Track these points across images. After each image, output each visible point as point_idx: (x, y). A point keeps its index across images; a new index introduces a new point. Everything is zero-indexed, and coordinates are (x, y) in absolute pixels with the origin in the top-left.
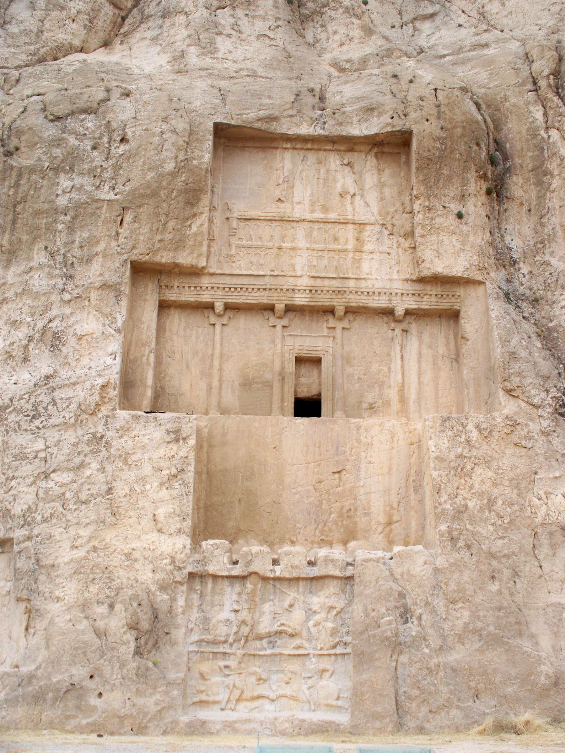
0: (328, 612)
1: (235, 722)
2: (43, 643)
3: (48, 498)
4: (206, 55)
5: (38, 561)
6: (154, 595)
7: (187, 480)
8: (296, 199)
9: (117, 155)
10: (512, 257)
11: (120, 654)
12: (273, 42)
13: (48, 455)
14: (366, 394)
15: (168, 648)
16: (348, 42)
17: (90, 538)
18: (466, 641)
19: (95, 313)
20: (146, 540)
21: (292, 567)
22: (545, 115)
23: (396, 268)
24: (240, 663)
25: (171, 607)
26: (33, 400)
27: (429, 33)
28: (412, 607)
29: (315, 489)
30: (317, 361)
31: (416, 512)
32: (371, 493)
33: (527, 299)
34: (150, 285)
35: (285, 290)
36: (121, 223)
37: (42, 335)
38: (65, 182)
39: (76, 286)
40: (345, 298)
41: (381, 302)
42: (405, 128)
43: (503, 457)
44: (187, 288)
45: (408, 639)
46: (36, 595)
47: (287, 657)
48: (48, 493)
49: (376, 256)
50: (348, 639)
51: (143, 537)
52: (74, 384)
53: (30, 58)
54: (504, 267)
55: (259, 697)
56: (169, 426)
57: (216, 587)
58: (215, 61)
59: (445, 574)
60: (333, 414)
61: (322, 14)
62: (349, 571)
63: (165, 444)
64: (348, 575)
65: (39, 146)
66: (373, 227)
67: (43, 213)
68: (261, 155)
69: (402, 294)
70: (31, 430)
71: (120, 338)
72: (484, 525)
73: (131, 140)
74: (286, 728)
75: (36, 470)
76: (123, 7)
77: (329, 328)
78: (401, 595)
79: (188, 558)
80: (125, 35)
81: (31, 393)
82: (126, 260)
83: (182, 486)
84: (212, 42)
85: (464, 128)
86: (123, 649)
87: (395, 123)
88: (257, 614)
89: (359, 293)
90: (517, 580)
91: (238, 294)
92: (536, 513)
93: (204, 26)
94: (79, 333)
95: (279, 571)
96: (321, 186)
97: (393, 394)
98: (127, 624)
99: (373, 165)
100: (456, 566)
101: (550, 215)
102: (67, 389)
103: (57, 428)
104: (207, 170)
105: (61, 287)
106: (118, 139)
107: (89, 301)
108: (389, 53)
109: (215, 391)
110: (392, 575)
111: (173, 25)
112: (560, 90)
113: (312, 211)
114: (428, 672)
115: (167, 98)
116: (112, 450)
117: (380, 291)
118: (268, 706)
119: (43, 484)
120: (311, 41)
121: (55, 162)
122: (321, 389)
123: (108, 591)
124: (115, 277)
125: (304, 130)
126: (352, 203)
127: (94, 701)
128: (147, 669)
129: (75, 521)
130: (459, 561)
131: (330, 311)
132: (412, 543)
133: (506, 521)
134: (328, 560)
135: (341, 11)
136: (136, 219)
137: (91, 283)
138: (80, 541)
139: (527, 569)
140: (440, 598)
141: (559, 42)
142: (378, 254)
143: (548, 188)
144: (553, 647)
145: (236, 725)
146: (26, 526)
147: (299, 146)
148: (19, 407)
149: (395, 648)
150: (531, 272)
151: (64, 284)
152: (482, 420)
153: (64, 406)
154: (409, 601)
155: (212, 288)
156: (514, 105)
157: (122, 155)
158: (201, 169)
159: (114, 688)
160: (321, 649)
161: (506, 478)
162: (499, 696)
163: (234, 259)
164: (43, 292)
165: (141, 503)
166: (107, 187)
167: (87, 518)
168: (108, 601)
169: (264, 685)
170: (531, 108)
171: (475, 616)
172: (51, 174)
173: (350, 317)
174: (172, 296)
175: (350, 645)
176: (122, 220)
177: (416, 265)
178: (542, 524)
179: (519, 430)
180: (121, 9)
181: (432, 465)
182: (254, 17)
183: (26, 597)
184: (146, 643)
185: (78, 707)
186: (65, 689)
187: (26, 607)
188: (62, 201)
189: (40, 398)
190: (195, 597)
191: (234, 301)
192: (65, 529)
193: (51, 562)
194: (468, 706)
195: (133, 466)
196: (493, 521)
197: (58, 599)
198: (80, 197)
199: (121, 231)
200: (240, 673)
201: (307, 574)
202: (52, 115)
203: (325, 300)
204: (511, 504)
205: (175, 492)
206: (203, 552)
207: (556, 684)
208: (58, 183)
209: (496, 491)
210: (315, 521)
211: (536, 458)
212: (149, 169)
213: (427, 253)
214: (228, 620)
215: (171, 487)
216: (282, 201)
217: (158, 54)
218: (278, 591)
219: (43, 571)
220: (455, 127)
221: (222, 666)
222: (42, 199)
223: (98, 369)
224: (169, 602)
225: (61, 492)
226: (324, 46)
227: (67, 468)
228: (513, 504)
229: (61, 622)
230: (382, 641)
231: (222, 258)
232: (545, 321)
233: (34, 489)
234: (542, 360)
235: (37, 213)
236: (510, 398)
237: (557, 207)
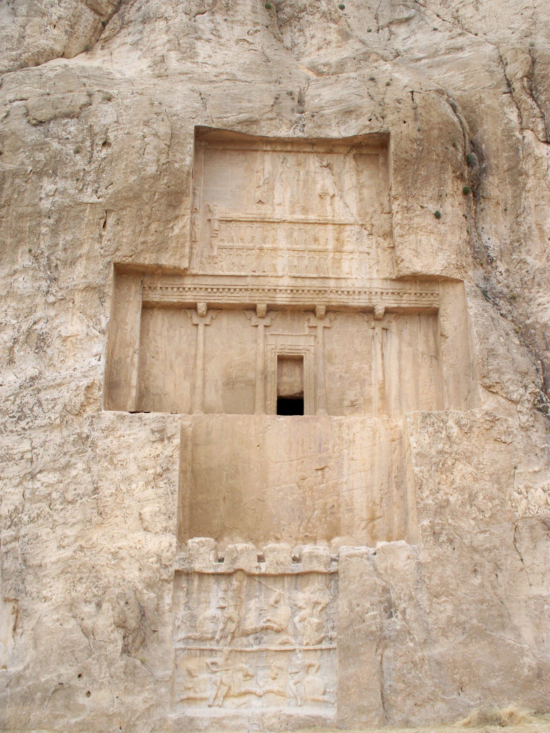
0: (314, 608)
1: (223, 718)
2: (31, 642)
3: (34, 498)
4: (186, 60)
5: (25, 561)
6: (141, 593)
7: (173, 479)
8: (276, 201)
9: (99, 159)
10: (489, 256)
11: (108, 653)
12: (252, 47)
13: (34, 455)
14: (348, 392)
15: (156, 646)
16: (325, 46)
17: (77, 538)
18: (450, 634)
19: (79, 314)
20: (133, 538)
21: (277, 563)
22: (520, 116)
23: (376, 268)
24: (227, 659)
25: (158, 605)
26: (18, 402)
27: (405, 37)
28: (396, 602)
29: (299, 486)
30: (299, 360)
31: (398, 507)
32: (353, 489)
33: (505, 296)
34: (133, 286)
35: (266, 290)
36: (104, 226)
37: (27, 337)
38: (48, 185)
39: (60, 289)
40: (326, 298)
41: (362, 301)
42: (382, 130)
43: (483, 452)
44: (170, 290)
45: (392, 634)
46: (24, 595)
47: (273, 653)
48: (34, 494)
49: (356, 256)
50: (333, 634)
51: (130, 536)
52: (60, 385)
53: (12, 63)
54: (482, 265)
55: (246, 693)
56: (154, 426)
57: (202, 585)
58: (195, 65)
59: (428, 568)
60: (315, 411)
61: (300, 18)
62: (334, 567)
63: (150, 443)
64: (332, 571)
65: (22, 150)
66: (352, 228)
67: (27, 216)
68: (242, 157)
69: (382, 293)
70: (17, 431)
71: (104, 339)
72: (465, 519)
73: (113, 144)
74: (274, 724)
75: (22, 470)
76: (103, 13)
77: (310, 327)
78: (386, 590)
79: (175, 556)
80: (106, 40)
81: (16, 395)
82: (110, 262)
83: (167, 485)
84: (192, 47)
85: (441, 129)
86: (110, 647)
87: (373, 125)
88: (243, 611)
89: (339, 292)
90: (499, 574)
91: (220, 295)
92: (516, 507)
93: (183, 31)
94: (64, 335)
95: (264, 568)
96: (301, 187)
97: (374, 392)
98: (114, 623)
99: (352, 166)
100: (439, 560)
101: (525, 214)
102: (52, 390)
103: (43, 429)
104: (189, 172)
105: (45, 289)
106: (101, 143)
107: (73, 302)
108: (366, 56)
109: (199, 391)
110: (376, 570)
111: (153, 30)
112: (534, 92)
113: (293, 213)
114: (412, 666)
115: (148, 102)
116: (97, 450)
117: (360, 290)
118: (255, 702)
119: (30, 485)
120: (289, 45)
121: (38, 166)
122: (303, 387)
123: (95, 590)
124: (99, 279)
125: (284, 132)
126: (331, 204)
127: (82, 700)
128: (135, 667)
129: (61, 521)
130: (442, 555)
131: (311, 311)
132: (395, 538)
133: (487, 516)
134: (312, 557)
135: (318, 15)
136: (119, 222)
137: (75, 285)
138: (66, 541)
139: (509, 562)
140: (424, 592)
141: (532, 45)
142: (358, 254)
143: (524, 188)
144: (536, 639)
145: (224, 722)
146: (13, 527)
147: (278, 148)
148: (4, 409)
149: (380, 642)
150: (508, 271)
151: (49, 286)
152: (462, 416)
153: (50, 407)
154: (393, 596)
155: (195, 289)
156: (489, 107)
157: (105, 158)
158: (182, 172)
159: (102, 687)
160: (307, 644)
161: (487, 473)
162: (484, 688)
163: (216, 260)
164: (27, 295)
165: (127, 502)
166: (90, 190)
167: (74, 517)
168: (96, 600)
169: (251, 681)
170: (506, 109)
171: (458, 609)
172: (34, 177)
173: (332, 316)
174: (155, 297)
175: (336, 640)
176: (105, 223)
177: (395, 264)
178: (522, 518)
179: (499, 425)
180: (101, 15)
181: (414, 461)
182: (232, 22)
183: (14, 597)
184: (134, 641)
185: (67, 707)
186: (53, 689)
187: (14, 608)
188: (46, 205)
189: (26, 400)
190: (182, 594)
191: (216, 301)
192: (52, 529)
193: (38, 562)
194: (453, 699)
195: (118, 466)
196: (474, 515)
197: (46, 599)
198: (64, 200)
199: (104, 233)
200: (227, 670)
201: (292, 571)
202: (34, 119)
203: (306, 300)
204: (492, 499)
205: (160, 491)
206: (189, 550)
207: (539, 676)
208: (42, 186)
209: (477, 485)
210: (299, 517)
211: (516, 453)
212: (131, 172)
213: (405, 253)
214: (214, 617)
215: (156, 486)
216: (263, 203)
217: (139, 59)
218: (263, 587)
219: (30, 571)
220: (431, 129)
221: (209, 664)
222: (26, 202)
223: (83, 370)
224: (156, 599)
225: (47, 492)
226: (302, 50)
227: (53, 468)
228: (494, 499)
229: (49, 622)
230: (367, 636)
231: (204, 259)
232: (522, 318)
233: (20, 489)
234: (520, 357)
235: (21, 216)
236: (490, 394)
237: (533, 206)
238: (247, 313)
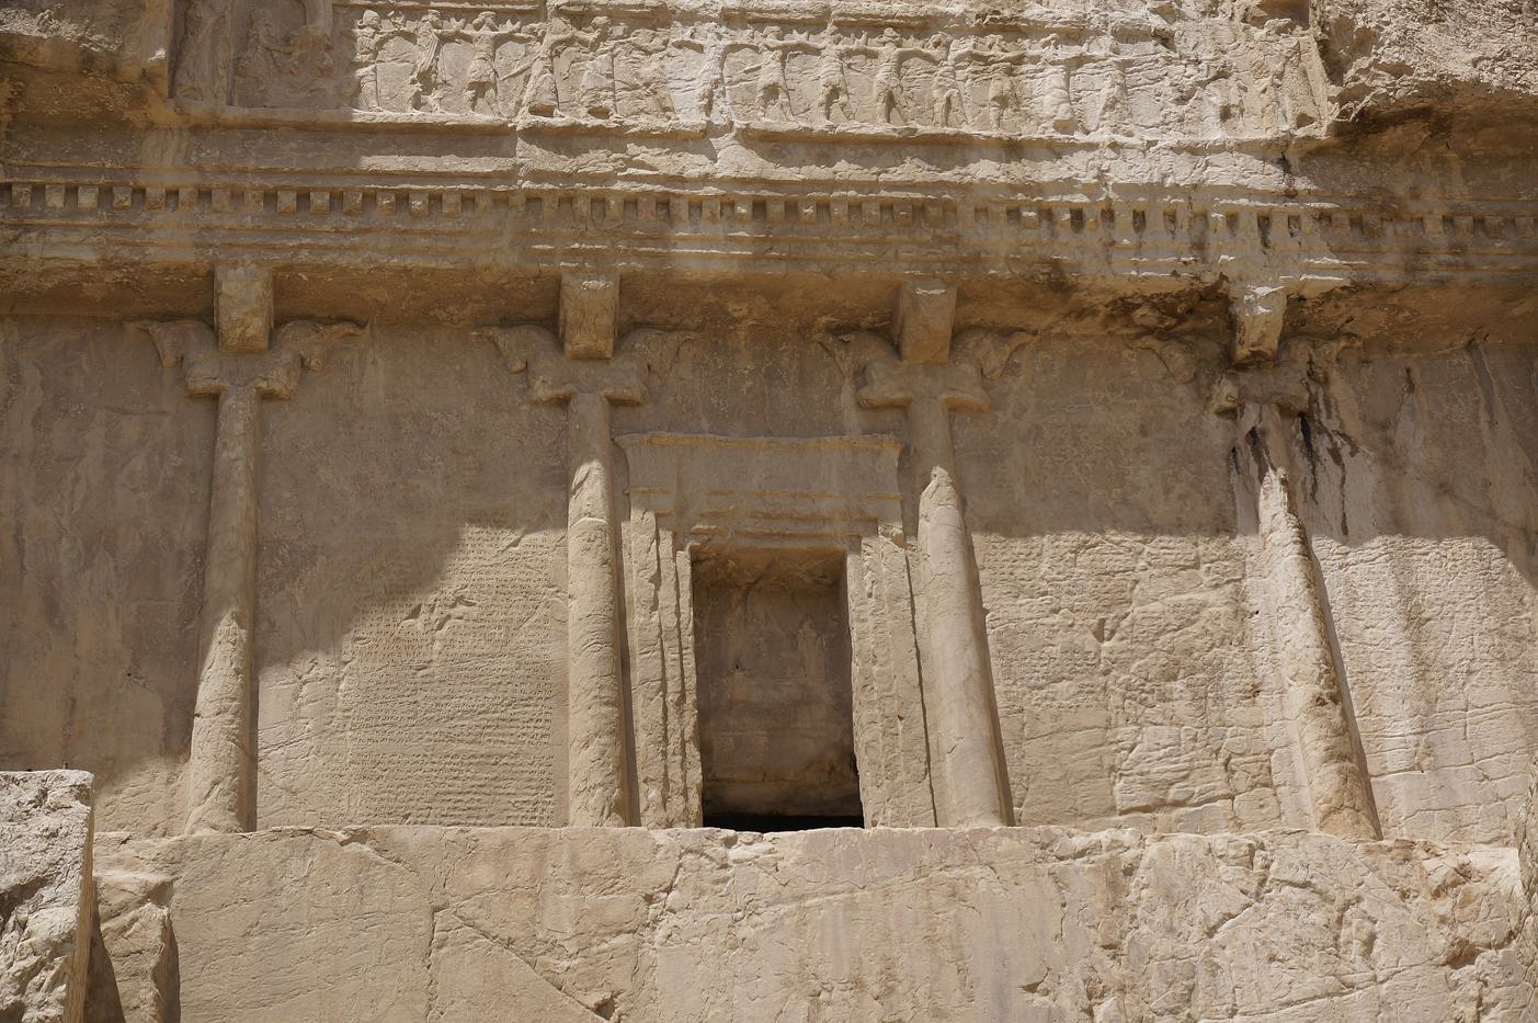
44: (56, 200)
238: (504, 339)
